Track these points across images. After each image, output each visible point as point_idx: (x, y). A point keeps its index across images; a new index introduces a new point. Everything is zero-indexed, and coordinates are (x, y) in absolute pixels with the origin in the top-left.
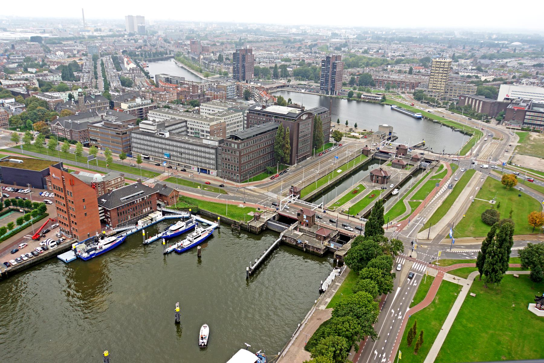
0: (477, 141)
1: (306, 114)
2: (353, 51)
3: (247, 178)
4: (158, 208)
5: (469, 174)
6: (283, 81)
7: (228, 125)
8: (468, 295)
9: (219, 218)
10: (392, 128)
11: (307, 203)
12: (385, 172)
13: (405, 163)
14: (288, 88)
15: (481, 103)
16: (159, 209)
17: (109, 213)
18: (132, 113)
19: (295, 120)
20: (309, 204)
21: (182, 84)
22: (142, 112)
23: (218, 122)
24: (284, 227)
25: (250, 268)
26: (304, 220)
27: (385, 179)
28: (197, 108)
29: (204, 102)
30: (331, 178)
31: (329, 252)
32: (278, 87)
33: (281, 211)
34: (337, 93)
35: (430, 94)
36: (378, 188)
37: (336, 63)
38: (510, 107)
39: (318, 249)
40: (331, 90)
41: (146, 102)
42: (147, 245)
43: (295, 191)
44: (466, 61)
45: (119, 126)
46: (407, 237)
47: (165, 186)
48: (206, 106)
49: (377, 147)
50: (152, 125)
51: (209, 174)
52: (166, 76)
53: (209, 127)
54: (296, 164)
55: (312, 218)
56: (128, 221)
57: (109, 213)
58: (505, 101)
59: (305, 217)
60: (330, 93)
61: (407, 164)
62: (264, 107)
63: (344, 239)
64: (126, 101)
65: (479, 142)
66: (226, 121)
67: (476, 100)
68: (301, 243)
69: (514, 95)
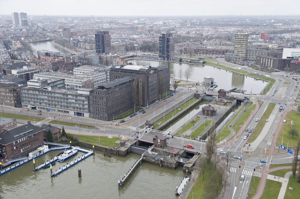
0: (273, 85)
1: (153, 69)
2: (179, 33)
3: (113, 117)
4: (45, 143)
5: (272, 106)
6: (131, 54)
7: (95, 82)
8: (288, 190)
9: (93, 146)
10: (213, 79)
11: (159, 132)
12: (213, 108)
13: (226, 101)
14: (136, 57)
15: (272, 60)
16: (46, 143)
17: (4, 148)
18: (21, 76)
19: (145, 74)
20: (161, 132)
21: (58, 56)
22: (28, 76)
23: (88, 79)
24: (144, 149)
25: (120, 181)
26: (159, 143)
27: (213, 113)
28: (71, 71)
29: (76, 67)
30: (174, 115)
31: (179, 165)
32: (129, 57)
33: (140, 139)
34: (171, 60)
35: (236, 57)
36: (209, 119)
37: (169, 38)
38: (292, 62)
39: (171, 164)
40: (167, 57)
41: (31, 68)
42: (37, 170)
43: (150, 124)
44: (257, 36)
45: (11, 85)
46: (235, 151)
47: (50, 126)
48: (78, 70)
49: (205, 92)
50: (37, 82)
51: (83, 116)
52: (46, 52)
53: (81, 83)
54: (148, 107)
55: (164, 141)
56: (21, 154)
57: (4, 148)
58: (288, 59)
59: (159, 141)
60: (166, 60)
61: (227, 102)
62: (122, 66)
63: (190, 155)
64: (15, 68)
65: (274, 85)
66: (94, 78)
67: (268, 59)
68: (158, 160)
69: (293, 55)
